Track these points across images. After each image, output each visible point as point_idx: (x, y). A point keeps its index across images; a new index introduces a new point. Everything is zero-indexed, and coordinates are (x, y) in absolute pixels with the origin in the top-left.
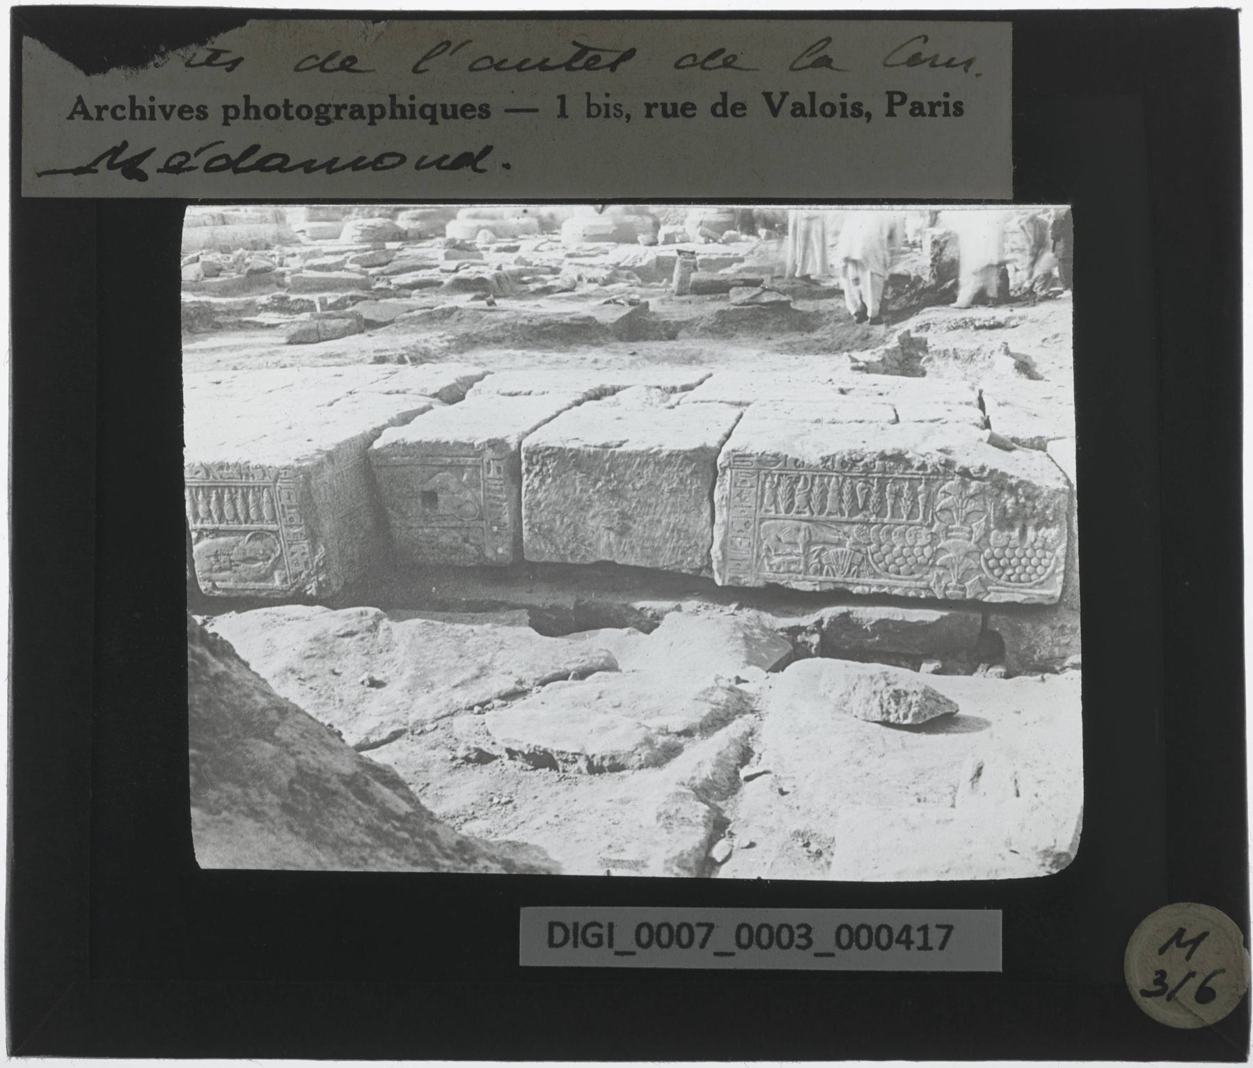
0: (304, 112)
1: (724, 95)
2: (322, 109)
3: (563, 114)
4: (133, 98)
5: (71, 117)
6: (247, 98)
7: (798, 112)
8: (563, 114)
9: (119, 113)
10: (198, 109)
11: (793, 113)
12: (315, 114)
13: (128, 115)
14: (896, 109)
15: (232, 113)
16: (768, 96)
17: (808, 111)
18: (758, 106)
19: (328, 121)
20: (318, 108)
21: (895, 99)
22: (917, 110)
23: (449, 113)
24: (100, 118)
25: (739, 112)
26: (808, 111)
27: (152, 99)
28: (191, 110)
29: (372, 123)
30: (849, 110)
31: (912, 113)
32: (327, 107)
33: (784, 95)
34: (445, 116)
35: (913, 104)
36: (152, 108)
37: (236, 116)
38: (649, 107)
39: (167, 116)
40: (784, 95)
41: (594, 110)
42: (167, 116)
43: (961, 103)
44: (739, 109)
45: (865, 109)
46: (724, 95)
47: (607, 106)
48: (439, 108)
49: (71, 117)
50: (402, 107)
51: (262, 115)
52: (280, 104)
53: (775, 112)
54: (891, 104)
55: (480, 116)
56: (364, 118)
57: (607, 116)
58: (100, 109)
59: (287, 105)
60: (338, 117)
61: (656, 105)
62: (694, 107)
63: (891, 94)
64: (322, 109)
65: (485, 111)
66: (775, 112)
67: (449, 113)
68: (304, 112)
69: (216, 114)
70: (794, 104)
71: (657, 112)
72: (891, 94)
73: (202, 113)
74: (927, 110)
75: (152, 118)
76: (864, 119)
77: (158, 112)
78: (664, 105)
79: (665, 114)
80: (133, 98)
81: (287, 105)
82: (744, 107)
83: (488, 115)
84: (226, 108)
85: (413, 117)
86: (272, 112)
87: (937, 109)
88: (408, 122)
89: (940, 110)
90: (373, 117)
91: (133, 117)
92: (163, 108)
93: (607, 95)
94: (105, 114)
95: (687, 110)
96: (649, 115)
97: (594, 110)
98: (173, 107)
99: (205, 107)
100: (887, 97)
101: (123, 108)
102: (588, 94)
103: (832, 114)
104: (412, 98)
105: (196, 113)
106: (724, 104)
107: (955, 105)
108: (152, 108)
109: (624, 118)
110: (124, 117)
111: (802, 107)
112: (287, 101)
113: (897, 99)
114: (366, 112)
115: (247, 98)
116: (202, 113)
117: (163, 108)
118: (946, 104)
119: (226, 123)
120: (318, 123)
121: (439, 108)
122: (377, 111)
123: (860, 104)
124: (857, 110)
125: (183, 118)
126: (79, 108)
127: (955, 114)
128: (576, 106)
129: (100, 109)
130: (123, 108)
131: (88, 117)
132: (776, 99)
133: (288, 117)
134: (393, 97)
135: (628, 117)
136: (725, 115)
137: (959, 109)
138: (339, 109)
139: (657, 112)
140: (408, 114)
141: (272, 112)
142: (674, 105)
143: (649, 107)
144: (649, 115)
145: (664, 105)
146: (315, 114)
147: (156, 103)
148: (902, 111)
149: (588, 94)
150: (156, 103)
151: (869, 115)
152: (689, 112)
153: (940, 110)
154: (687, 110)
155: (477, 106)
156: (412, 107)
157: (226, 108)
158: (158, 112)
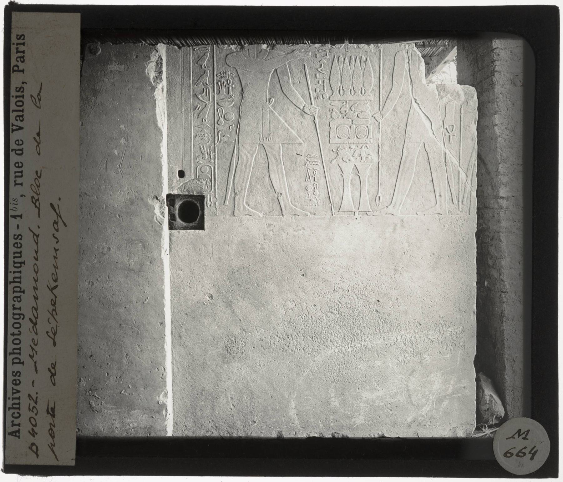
8: (21, 216)
9: (17, 415)
13: (18, 410)
14: (21, 68)
31: (23, 62)
36: (13, 399)
39: (18, 392)
42: (18, 392)
51: (18, 347)
54: (19, 71)
76: (25, 85)
77: (16, 396)
87: (19, 50)
89: (21, 48)
94: (16, 421)
98: (13, 389)
108: (13, 399)
118: (18, 44)
125: (19, 384)
153: (21, 48)
158: (16, 396)
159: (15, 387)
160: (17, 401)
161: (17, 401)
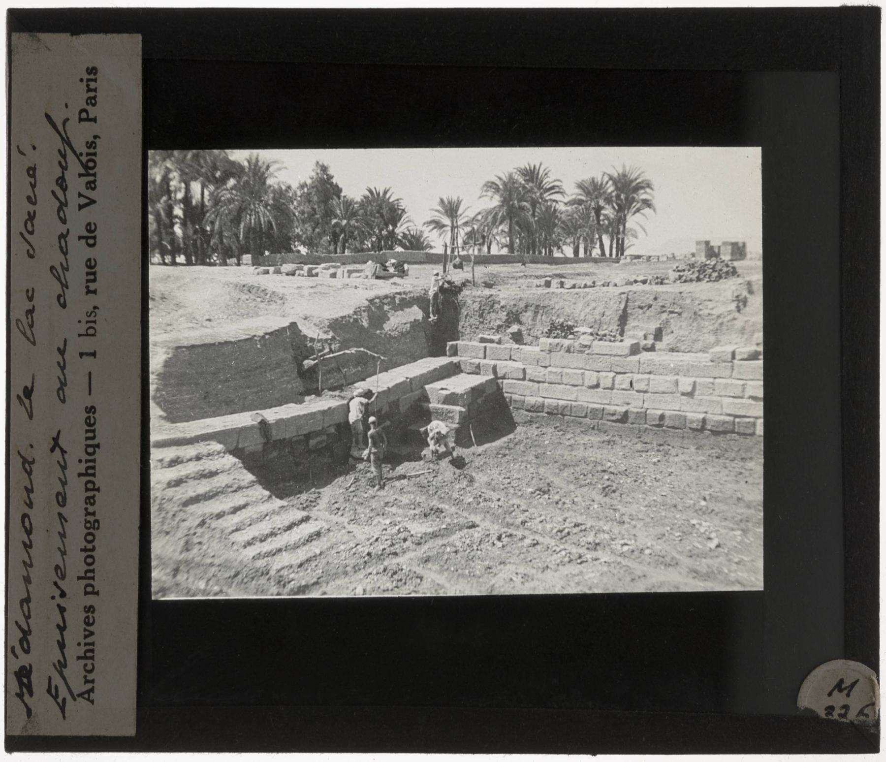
0: (90, 537)
1: (80, 238)
2: (88, 525)
3: (94, 354)
4: (79, 658)
5: (92, 702)
6: (79, 578)
7: (93, 185)
8: (94, 354)
9: (89, 667)
10: (87, 612)
11: (94, 189)
12: (92, 530)
13: (91, 661)
14: (91, 116)
15: (89, 589)
16: (81, 207)
17: (91, 178)
18: (88, 215)
19: (97, 521)
20: (87, 528)
21: (85, 117)
22: (92, 101)
23: (91, 435)
24: (93, 681)
25: (93, 227)
26: (91, 178)
27: (79, 644)
28: (88, 617)
29: (98, 490)
30: (92, 151)
31: (94, 105)
32: (87, 522)
33: (80, 195)
34: (93, 438)
35: (88, 104)
36: (86, 644)
37: (92, 586)
38: (89, 292)
39: (92, 633)
40: (80, 195)
41: (91, 331)
42: (92, 633)
43: (88, 69)
44: (91, 228)
45: (91, 139)
46: (80, 238)
47: (87, 322)
48: (90, 442)
49: (92, 702)
50: (88, 468)
51: (91, 568)
52: (85, 554)
53: (93, 202)
54: (88, 119)
55: (94, 413)
56: (94, 496)
57: (95, 322)
58: (87, 681)
59: (84, 550)
60: (93, 514)
61: (87, 287)
62: (89, 260)
63: (81, 120)
64: (88, 525)
65: (91, 410)
66: (93, 202)
67: (91, 435)
68: (90, 538)
69: (90, 600)
70: (87, 188)
71: (92, 286)
72: (81, 120)
73: (90, 609)
74: (92, 94)
75: (93, 644)
76: (97, 141)
77: (89, 640)
78: (88, 281)
79: (94, 280)
80: (79, 658)
81: (84, 550)
82: (89, 224)
83: (93, 407)
84: (86, 593)
85: (94, 461)
86: (90, 560)
88: (97, 465)
89: (92, 85)
90: (93, 489)
91: (92, 658)
92: (86, 637)
93: (80, 322)
94: (90, 677)
95: (91, 265)
96: (95, 292)
97: (91, 331)
98: (85, 630)
99: (85, 607)
100: (82, 123)
101: (86, 665)
102: (80, 335)
103: (94, 161)
104: (80, 461)
105: (90, 614)
106: (87, 238)
107: (89, 74)
108: (86, 644)
109: (96, 310)
110: (93, 664)
111: (89, 183)
112: (82, 550)
113: (84, 115)
114: (90, 494)
115: (79, 578)
116: (90, 609)
117: (86, 637)
118: (88, 80)
119: (97, 593)
120: (98, 528)
121: (90, 442)
122: (90, 486)
123: (87, 143)
124: (91, 145)
126: (86, 696)
127: (95, 74)
128: (88, 345)
129: (87, 681)
130: (86, 665)
131: (92, 690)
132: (83, 201)
133: (93, 549)
134: (80, 475)
135: (95, 308)
136: (94, 238)
137: (92, 71)
138: (88, 514)
139: (92, 286)
140: (91, 464)
141: (90, 560)
142: (88, 274)
143: (89, 292)
144: (95, 292)
145: (88, 281)
146: (92, 530)
147: (83, 641)
148: (93, 112)
149: (80, 335)
150: (83, 641)
151: (95, 137)
152: (93, 264)
153: (92, 85)
154: (91, 265)
155: (87, 415)
156: (87, 461)
157: (86, 593)
158: (89, 640)
159: (88, 628)
160: (91, 647)
161: (91, 647)
